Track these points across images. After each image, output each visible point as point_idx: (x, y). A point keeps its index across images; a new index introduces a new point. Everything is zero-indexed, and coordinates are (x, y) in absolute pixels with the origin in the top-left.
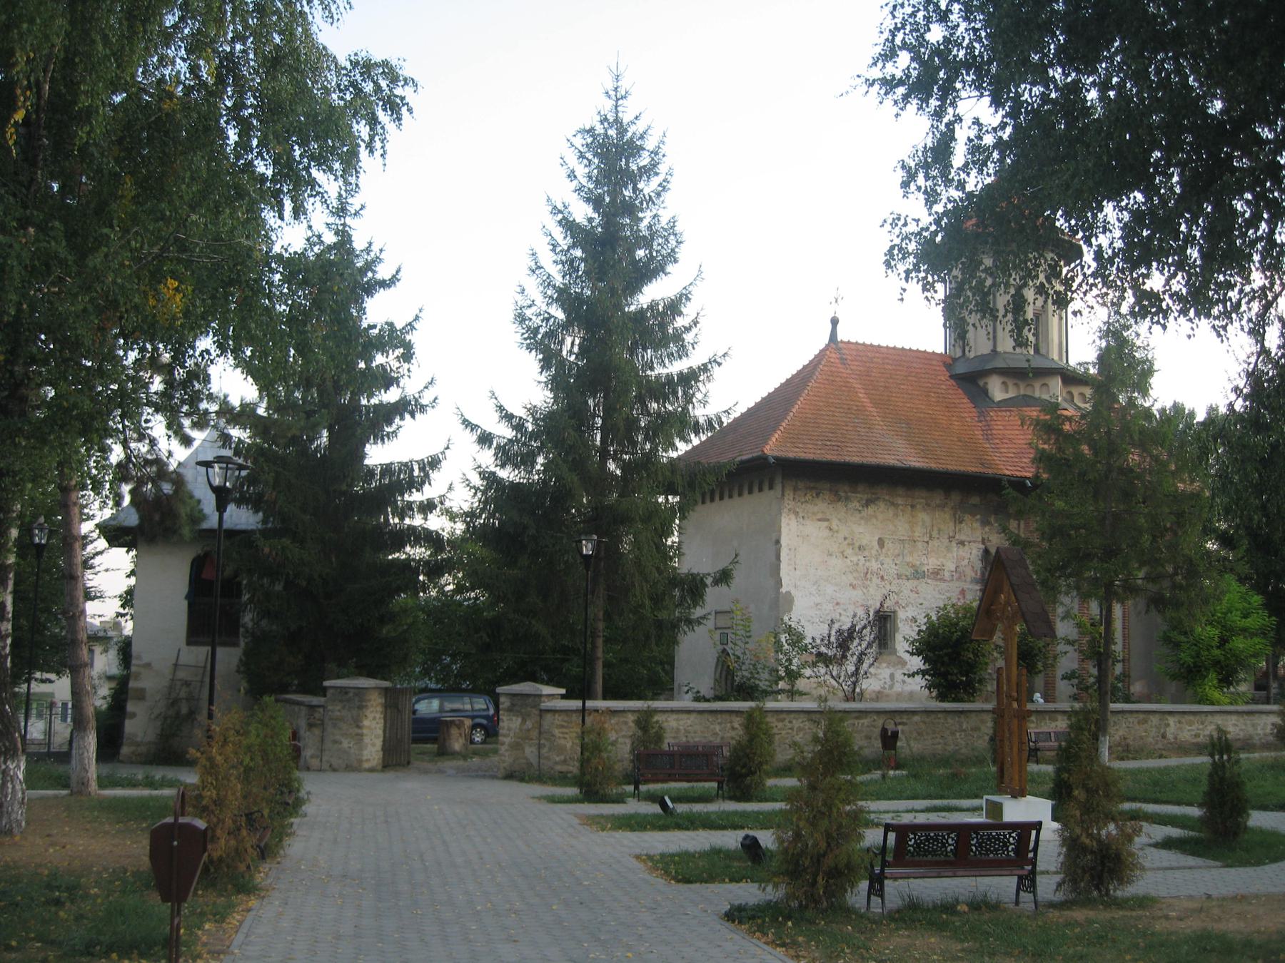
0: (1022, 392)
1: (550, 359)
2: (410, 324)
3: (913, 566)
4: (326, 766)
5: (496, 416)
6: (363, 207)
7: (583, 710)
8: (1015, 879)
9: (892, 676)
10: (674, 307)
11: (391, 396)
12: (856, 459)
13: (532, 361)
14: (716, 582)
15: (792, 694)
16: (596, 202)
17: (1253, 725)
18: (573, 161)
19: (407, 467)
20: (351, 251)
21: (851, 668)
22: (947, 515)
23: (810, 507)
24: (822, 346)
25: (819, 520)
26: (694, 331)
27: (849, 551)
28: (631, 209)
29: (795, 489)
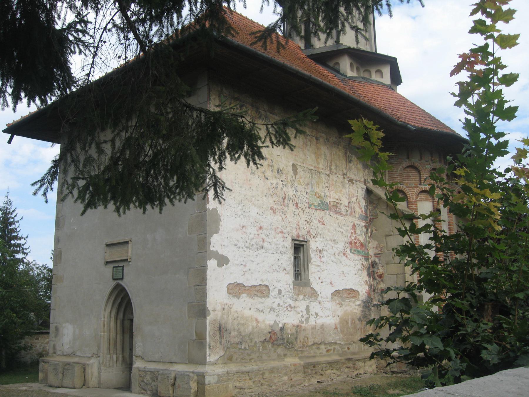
0: (362, 75)
3: (319, 197)
9: (307, 308)
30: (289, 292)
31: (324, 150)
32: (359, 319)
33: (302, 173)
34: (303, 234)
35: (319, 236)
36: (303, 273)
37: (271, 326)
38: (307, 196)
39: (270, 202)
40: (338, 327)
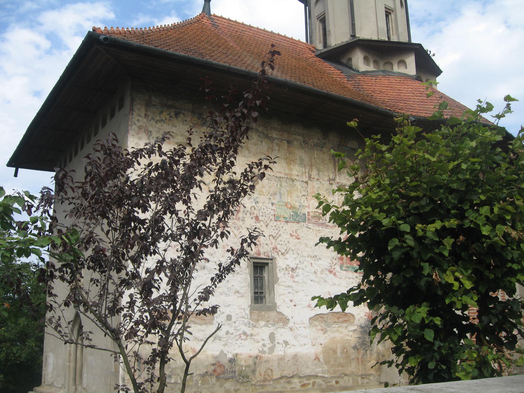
0: (382, 68)
3: (292, 207)
9: (272, 337)
29: (148, 105)
30: (243, 317)
31: (300, 153)
32: (355, 348)
35: (290, 252)
36: (267, 296)
37: (216, 358)
38: (273, 208)
40: (321, 357)
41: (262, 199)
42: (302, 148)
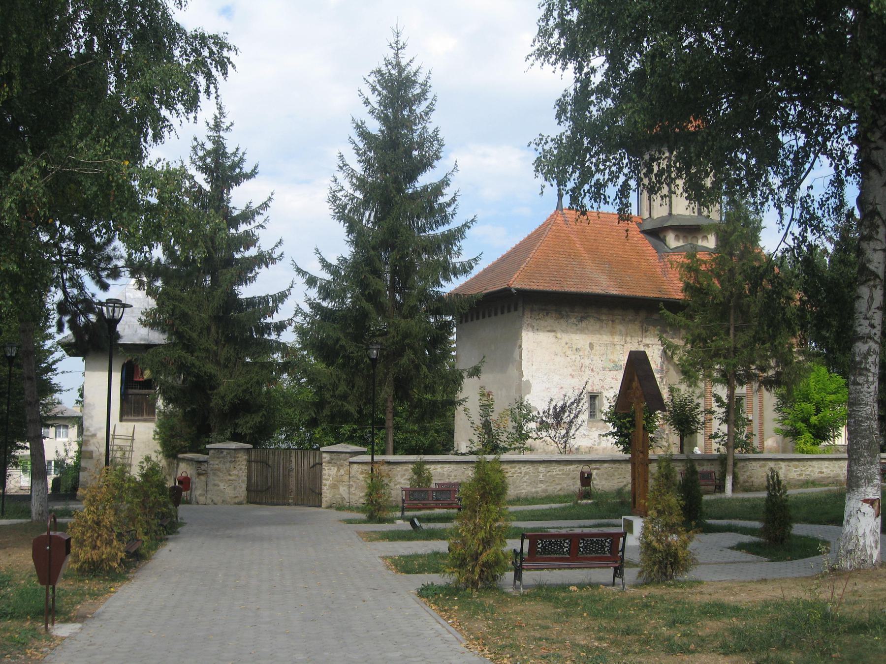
1: (353, 227)
2: (265, 203)
4: (209, 501)
5: (320, 266)
6: (232, 124)
7: (373, 462)
8: (612, 569)
10: (437, 189)
11: (252, 252)
12: (573, 290)
13: (341, 229)
14: (471, 375)
15: (521, 450)
16: (384, 119)
17: (840, 467)
18: (367, 92)
19: (264, 300)
20: (224, 154)
21: (563, 432)
22: (637, 327)
23: (543, 323)
24: (552, 212)
25: (549, 331)
26: (453, 206)
27: (569, 353)
28: (408, 124)
29: (532, 311)
31: (620, 327)
33: (598, 348)
34: (596, 389)
39: (570, 370)
41: (595, 358)
42: (621, 323)
